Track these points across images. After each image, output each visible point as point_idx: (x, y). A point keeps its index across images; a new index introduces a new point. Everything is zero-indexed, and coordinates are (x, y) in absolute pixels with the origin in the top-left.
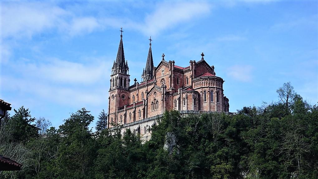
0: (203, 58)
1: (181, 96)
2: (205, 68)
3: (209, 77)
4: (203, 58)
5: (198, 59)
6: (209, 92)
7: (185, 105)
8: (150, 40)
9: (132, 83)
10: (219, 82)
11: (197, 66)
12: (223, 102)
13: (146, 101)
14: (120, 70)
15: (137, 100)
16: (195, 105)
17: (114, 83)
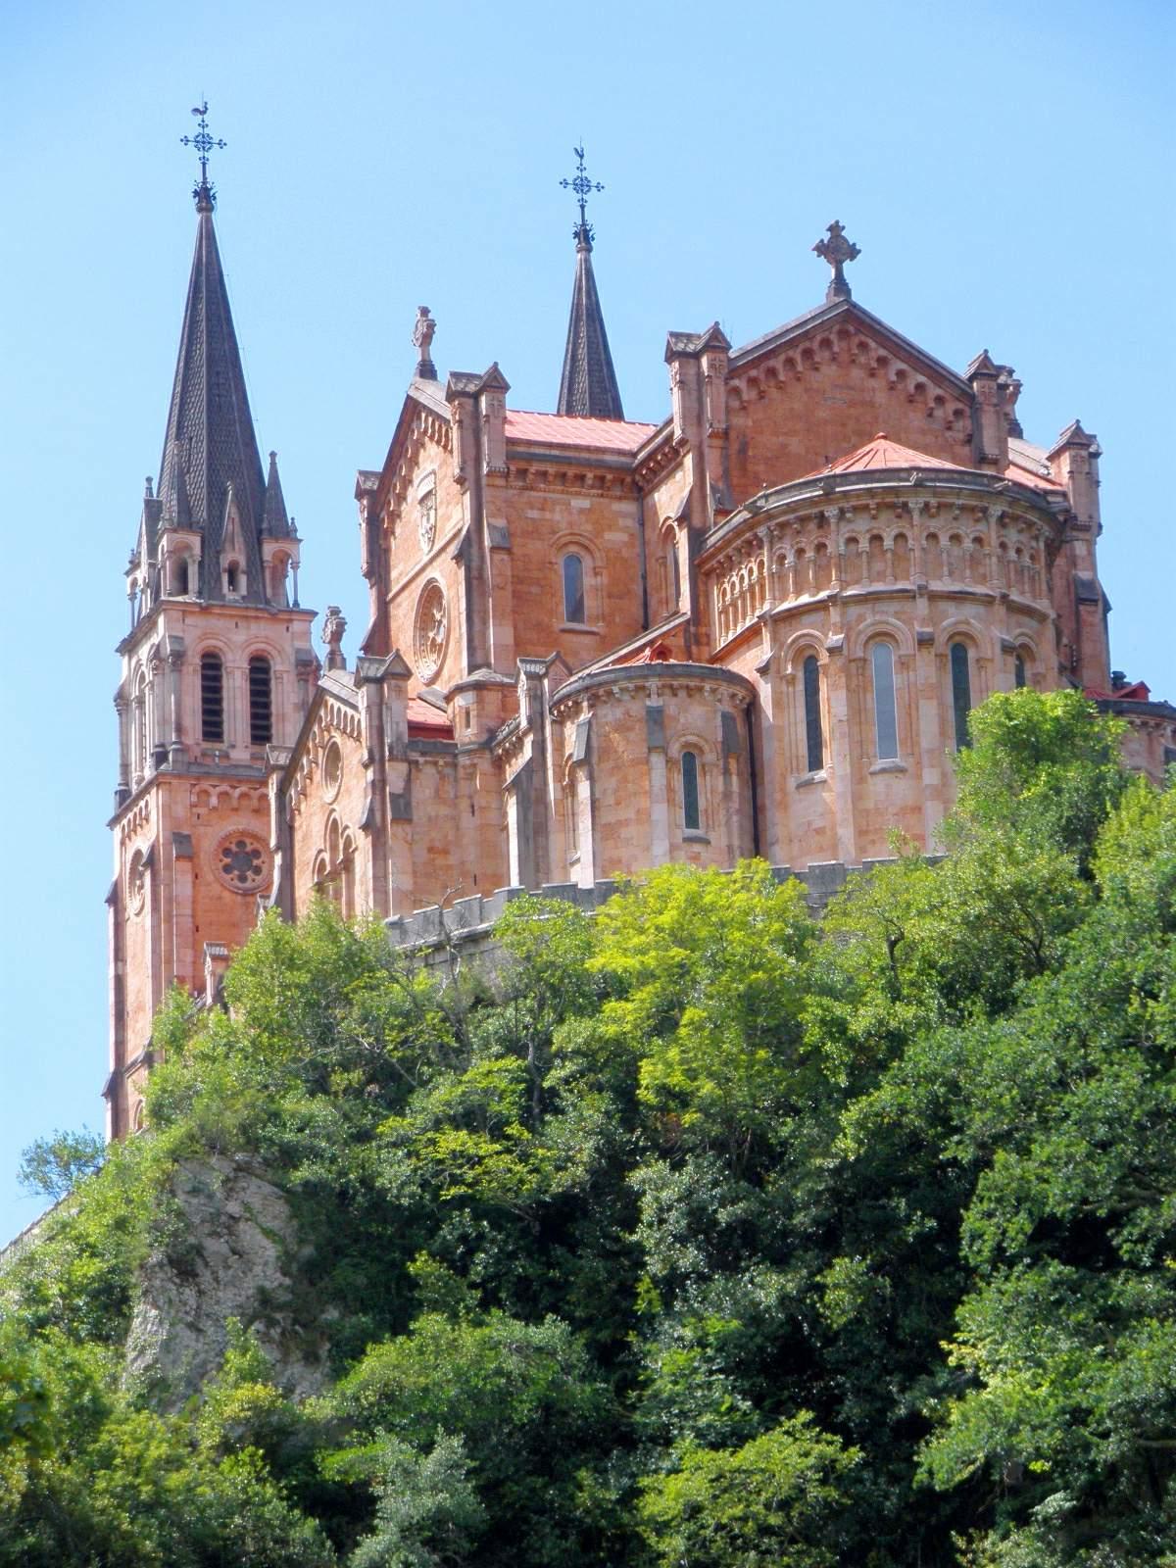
0: (840, 285)
2: (881, 398)
3: (828, 496)
4: (840, 285)
6: (839, 661)
8: (582, 185)
10: (968, 529)
14: (193, 571)
16: (692, 820)
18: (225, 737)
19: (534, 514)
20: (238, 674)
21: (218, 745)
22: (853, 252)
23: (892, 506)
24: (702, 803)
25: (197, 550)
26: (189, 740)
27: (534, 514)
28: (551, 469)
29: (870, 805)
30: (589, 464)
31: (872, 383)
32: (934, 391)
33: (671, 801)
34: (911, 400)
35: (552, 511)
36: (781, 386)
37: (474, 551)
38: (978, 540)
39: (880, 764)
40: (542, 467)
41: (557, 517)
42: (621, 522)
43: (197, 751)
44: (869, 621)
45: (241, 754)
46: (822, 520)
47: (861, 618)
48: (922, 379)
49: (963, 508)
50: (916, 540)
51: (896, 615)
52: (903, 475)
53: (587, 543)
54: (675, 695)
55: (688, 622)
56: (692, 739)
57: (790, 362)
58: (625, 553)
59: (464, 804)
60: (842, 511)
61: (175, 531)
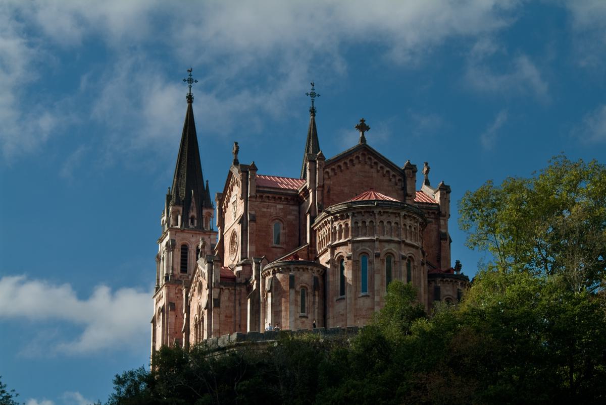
0: (363, 139)
2: (375, 175)
4: (363, 139)
10: (394, 220)
14: (180, 217)
16: (303, 310)
18: (188, 272)
19: (265, 210)
20: (193, 252)
21: (185, 274)
22: (368, 128)
23: (369, 212)
25: (181, 212)
26: (175, 273)
27: (265, 210)
28: (270, 196)
29: (358, 307)
30: (283, 194)
31: (373, 170)
32: (392, 173)
33: (296, 305)
34: (384, 176)
35: (270, 209)
36: (341, 171)
37: (245, 221)
38: (396, 223)
39: (362, 294)
40: (268, 195)
41: (272, 211)
42: (293, 213)
43: (178, 276)
44: (360, 249)
47: (358, 248)
48: (388, 169)
49: (392, 213)
50: (377, 223)
51: (369, 247)
52: (373, 202)
53: (281, 219)
54: (299, 271)
55: (308, 246)
56: (304, 285)
58: (294, 222)
59: (237, 302)
60: (353, 213)
61: (174, 206)
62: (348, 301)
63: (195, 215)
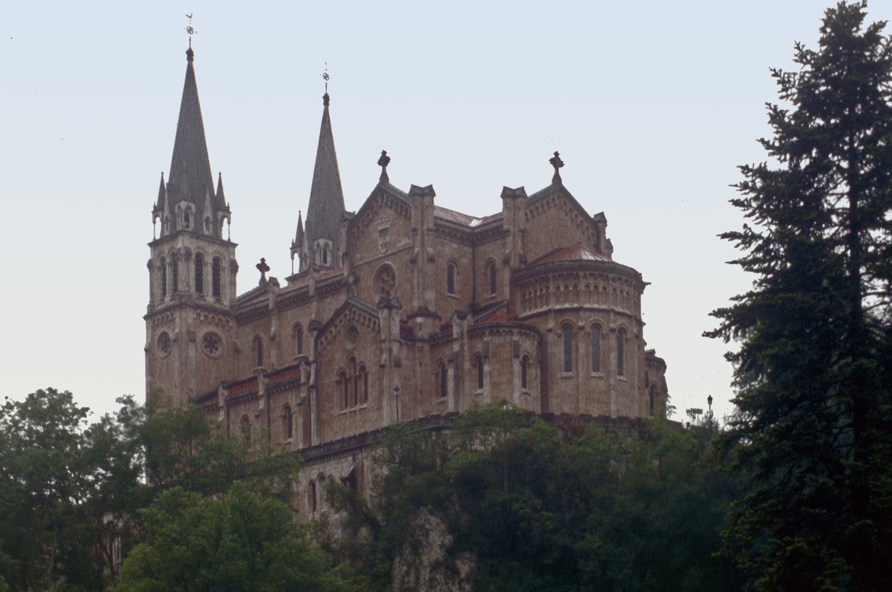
0: (557, 179)
1: (466, 348)
4: (557, 179)
5: (536, 182)
7: (481, 386)
9: (246, 282)
10: (626, 288)
11: (531, 211)
12: (643, 374)
13: (313, 366)
15: (274, 360)
16: (524, 386)
17: (164, 279)
22: (562, 165)
24: (528, 379)
31: (568, 218)
45: (210, 299)
46: (578, 277)
50: (610, 290)
57: (542, 206)
62: (581, 380)
63: (211, 217)
